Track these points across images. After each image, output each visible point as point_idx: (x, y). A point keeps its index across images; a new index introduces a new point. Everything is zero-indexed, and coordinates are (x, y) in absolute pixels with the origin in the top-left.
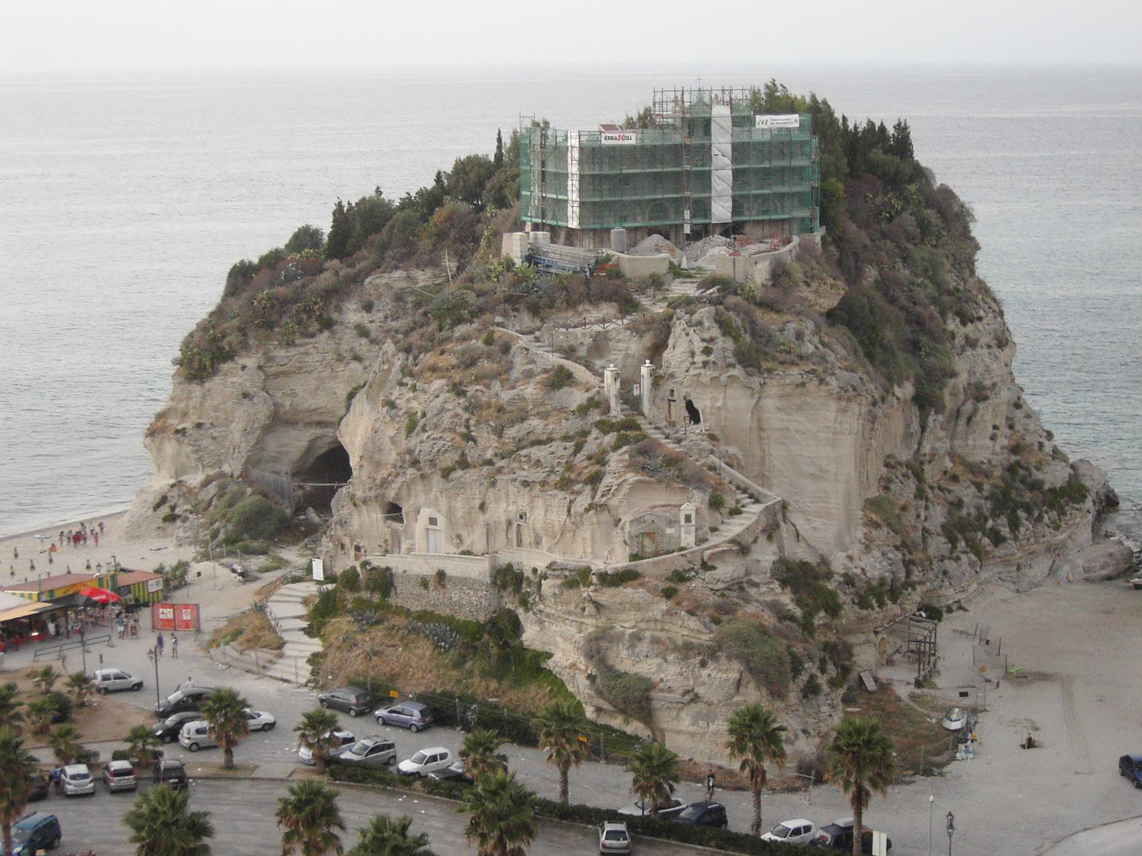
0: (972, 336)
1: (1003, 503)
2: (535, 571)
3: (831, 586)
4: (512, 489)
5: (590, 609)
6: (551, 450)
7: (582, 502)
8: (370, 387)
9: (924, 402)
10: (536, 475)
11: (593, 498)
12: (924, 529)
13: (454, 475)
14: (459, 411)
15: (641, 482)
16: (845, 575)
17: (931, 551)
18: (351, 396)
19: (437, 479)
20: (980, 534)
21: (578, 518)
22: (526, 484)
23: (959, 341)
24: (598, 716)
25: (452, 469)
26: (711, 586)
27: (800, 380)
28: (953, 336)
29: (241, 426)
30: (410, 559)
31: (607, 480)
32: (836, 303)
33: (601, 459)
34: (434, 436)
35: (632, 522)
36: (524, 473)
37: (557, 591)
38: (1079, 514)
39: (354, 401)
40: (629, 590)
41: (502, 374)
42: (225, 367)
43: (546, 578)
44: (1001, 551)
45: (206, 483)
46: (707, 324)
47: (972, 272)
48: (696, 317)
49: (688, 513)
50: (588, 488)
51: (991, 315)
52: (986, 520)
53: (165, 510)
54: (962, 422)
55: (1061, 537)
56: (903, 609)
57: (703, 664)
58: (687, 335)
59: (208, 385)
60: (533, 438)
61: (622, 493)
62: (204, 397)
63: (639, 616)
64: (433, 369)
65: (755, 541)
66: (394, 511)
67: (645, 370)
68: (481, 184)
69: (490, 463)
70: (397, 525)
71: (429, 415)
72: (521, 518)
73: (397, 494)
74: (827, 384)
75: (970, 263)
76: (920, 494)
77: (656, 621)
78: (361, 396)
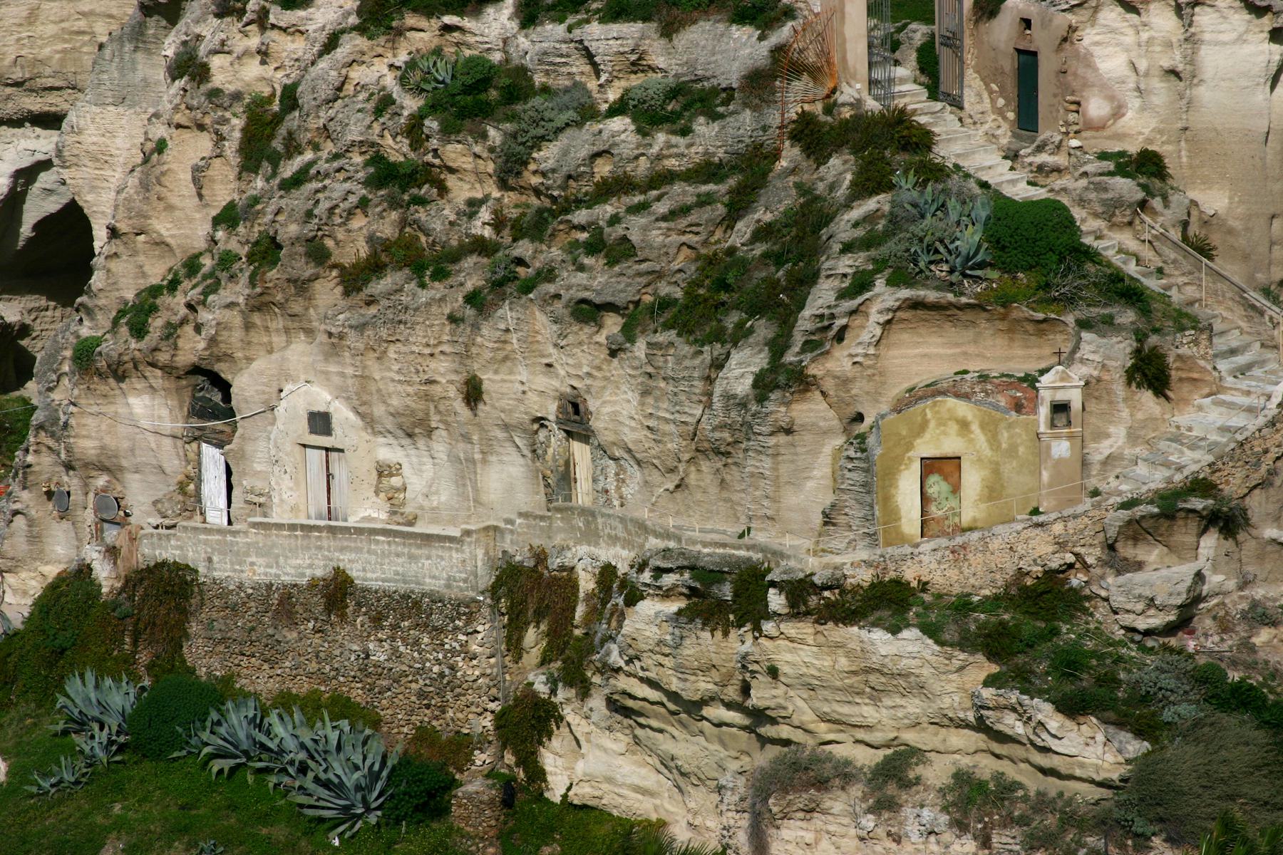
15: (916, 305)
19: (327, 292)
25: (373, 267)
26: (1127, 620)
36: (581, 278)
40: (879, 635)
49: (1061, 396)
50: (763, 329)
60: (603, 169)
61: (865, 337)
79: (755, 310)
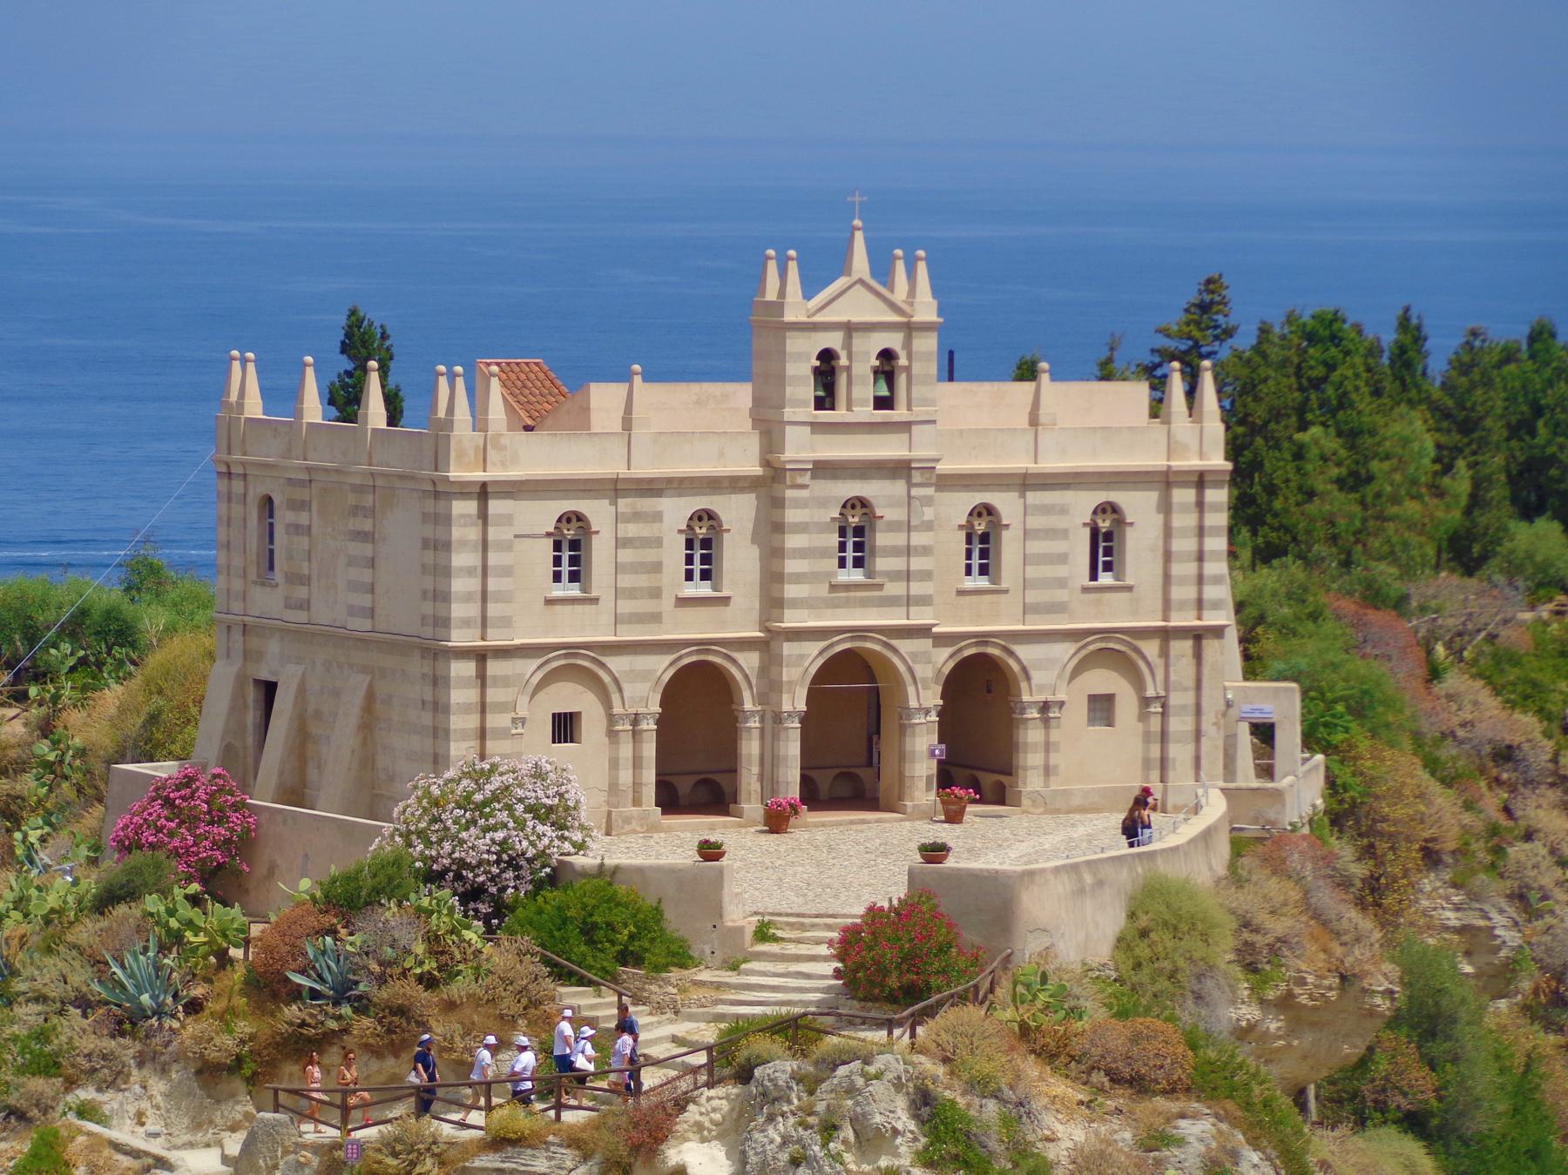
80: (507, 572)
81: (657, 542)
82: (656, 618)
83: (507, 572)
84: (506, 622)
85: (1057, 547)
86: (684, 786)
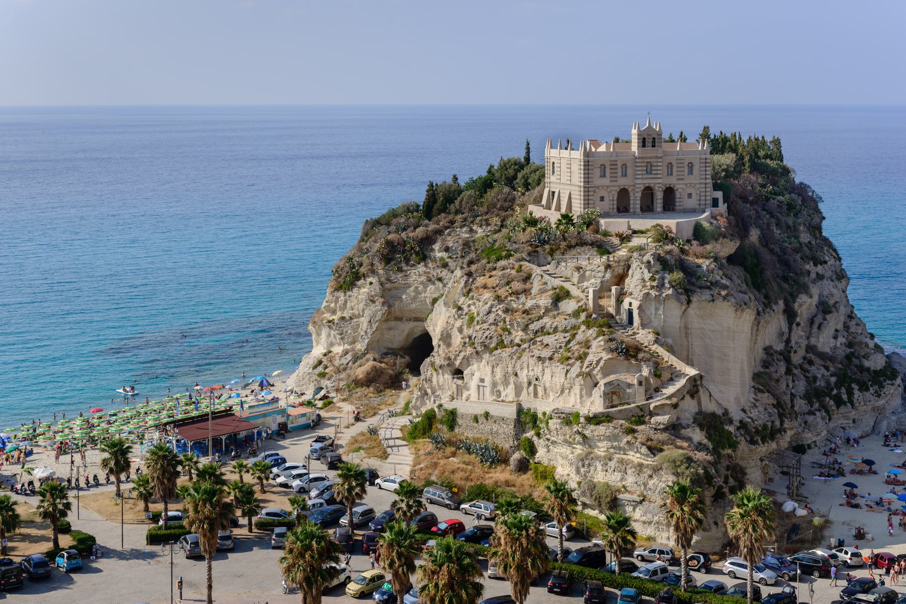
0: (820, 272)
1: (844, 380)
2: (544, 414)
3: (731, 429)
4: (532, 361)
5: (578, 438)
6: (556, 338)
7: (575, 370)
8: (446, 296)
9: (790, 315)
10: (546, 353)
11: (581, 367)
12: (792, 394)
13: (496, 352)
14: (500, 312)
16: (741, 422)
17: (796, 408)
18: (435, 301)
20: (828, 399)
21: (572, 381)
22: (539, 358)
23: (813, 276)
24: (583, 509)
27: (711, 299)
28: (809, 273)
29: (368, 319)
30: (467, 404)
31: (590, 358)
32: (732, 251)
33: (587, 345)
34: (485, 327)
35: (605, 384)
37: (558, 427)
38: (893, 388)
39: (436, 305)
41: (526, 292)
42: (359, 283)
43: (551, 418)
44: (842, 409)
45: (346, 353)
46: (652, 262)
47: (821, 233)
48: (645, 259)
50: (578, 363)
51: (833, 260)
52: (832, 390)
53: (320, 369)
54: (815, 327)
55: (881, 402)
56: (778, 445)
57: (651, 477)
58: (641, 269)
59: (349, 293)
62: (346, 302)
63: (609, 444)
64: (485, 287)
65: (683, 399)
66: (458, 373)
67: (614, 288)
68: (515, 177)
69: (519, 346)
70: (460, 382)
71: (481, 315)
72: (537, 379)
73: (461, 363)
74: (728, 301)
75: (819, 229)
76: (788, 372)
77: (620, 449)
78: (441, 302)
79: (577, 359)
80: (592, 174)
81: (617, 169)
82: (616, 181)
83: (592, 174)
84: (592, 182)
85: (682, 169)
86: (621, 209)
